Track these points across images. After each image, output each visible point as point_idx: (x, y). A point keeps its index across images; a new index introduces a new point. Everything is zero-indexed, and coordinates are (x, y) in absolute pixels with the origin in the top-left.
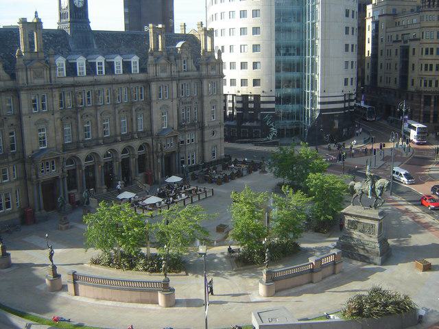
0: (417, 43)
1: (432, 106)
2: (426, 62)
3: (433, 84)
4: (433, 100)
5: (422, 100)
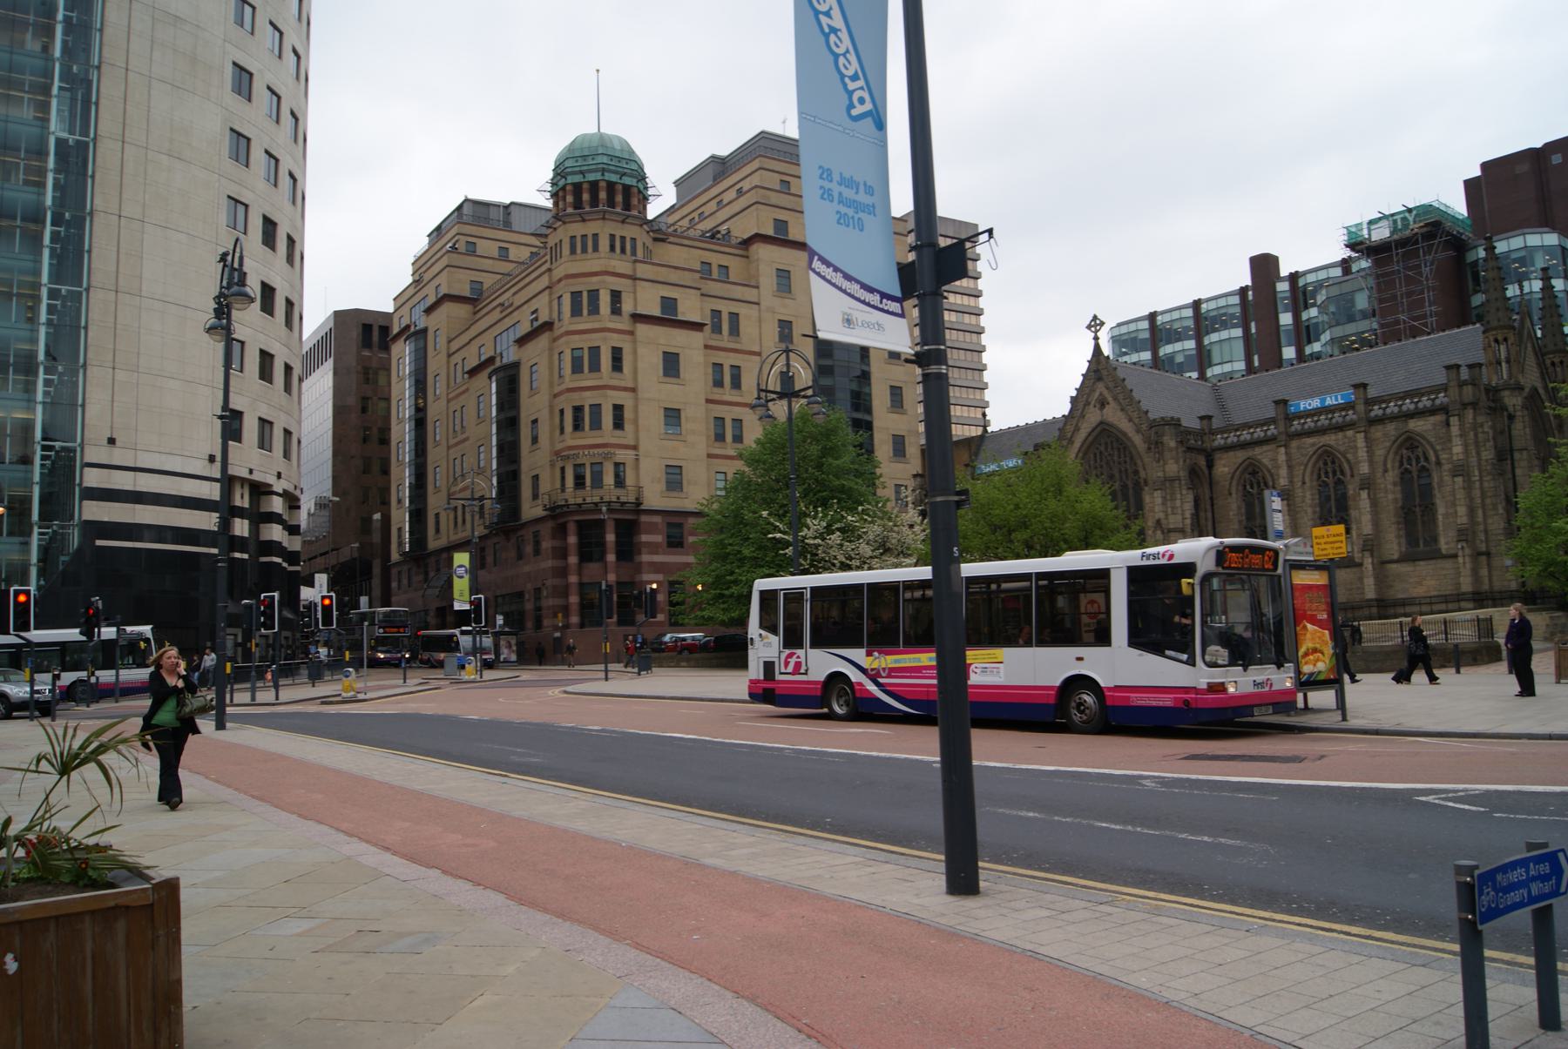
0: (543, 340)
1: (611, 557)
2: (577, 399)
3: (609, 479)
4: (610, 537)
5: (572, 539)
